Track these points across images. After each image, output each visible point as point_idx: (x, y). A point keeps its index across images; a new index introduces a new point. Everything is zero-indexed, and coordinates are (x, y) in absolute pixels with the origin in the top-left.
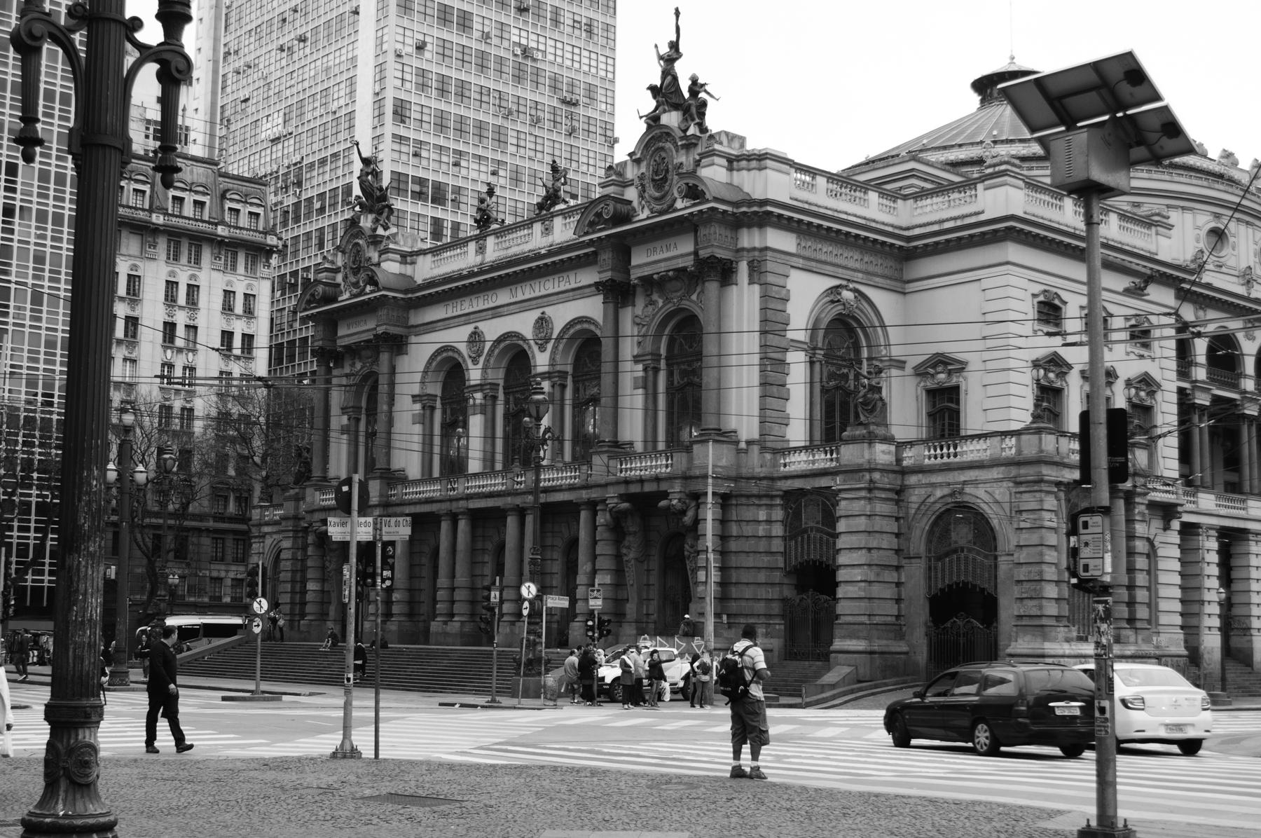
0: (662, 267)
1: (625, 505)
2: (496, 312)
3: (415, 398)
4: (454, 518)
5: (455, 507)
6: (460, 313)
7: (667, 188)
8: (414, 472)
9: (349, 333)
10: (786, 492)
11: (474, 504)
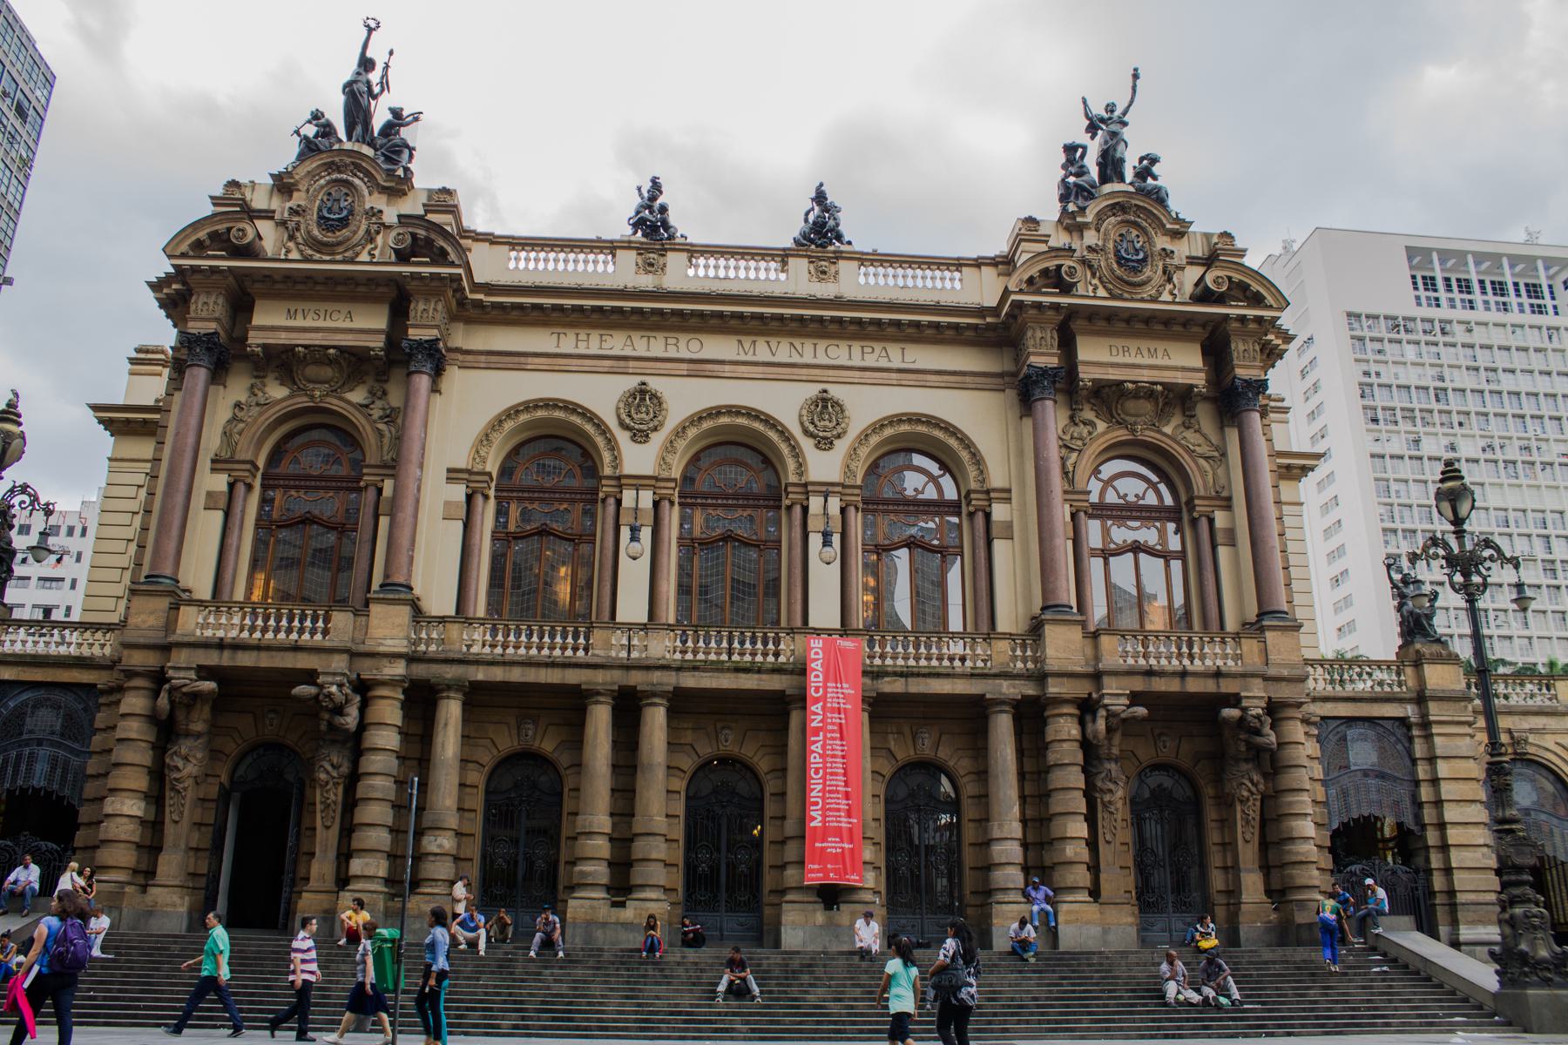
0: (1145, 376)
1: (1141, 711)
2: (699, 368)
3: (453, 475)
4: (628, 707)
5: (636, 679)
6: (594, 350)
7: (1147, 272)
8: (441, 601)
9: (273, 322)
10: (1323, 718)
11: (689, 681)
